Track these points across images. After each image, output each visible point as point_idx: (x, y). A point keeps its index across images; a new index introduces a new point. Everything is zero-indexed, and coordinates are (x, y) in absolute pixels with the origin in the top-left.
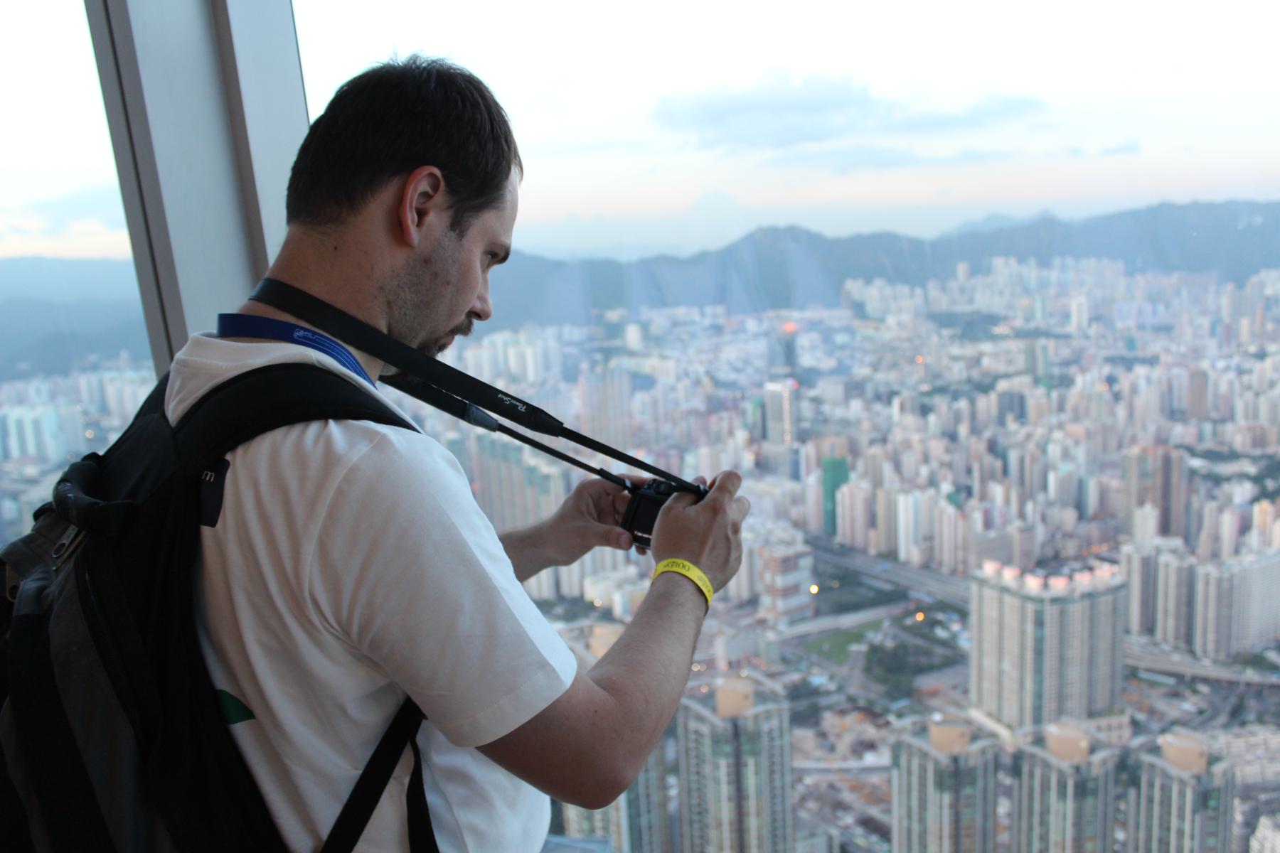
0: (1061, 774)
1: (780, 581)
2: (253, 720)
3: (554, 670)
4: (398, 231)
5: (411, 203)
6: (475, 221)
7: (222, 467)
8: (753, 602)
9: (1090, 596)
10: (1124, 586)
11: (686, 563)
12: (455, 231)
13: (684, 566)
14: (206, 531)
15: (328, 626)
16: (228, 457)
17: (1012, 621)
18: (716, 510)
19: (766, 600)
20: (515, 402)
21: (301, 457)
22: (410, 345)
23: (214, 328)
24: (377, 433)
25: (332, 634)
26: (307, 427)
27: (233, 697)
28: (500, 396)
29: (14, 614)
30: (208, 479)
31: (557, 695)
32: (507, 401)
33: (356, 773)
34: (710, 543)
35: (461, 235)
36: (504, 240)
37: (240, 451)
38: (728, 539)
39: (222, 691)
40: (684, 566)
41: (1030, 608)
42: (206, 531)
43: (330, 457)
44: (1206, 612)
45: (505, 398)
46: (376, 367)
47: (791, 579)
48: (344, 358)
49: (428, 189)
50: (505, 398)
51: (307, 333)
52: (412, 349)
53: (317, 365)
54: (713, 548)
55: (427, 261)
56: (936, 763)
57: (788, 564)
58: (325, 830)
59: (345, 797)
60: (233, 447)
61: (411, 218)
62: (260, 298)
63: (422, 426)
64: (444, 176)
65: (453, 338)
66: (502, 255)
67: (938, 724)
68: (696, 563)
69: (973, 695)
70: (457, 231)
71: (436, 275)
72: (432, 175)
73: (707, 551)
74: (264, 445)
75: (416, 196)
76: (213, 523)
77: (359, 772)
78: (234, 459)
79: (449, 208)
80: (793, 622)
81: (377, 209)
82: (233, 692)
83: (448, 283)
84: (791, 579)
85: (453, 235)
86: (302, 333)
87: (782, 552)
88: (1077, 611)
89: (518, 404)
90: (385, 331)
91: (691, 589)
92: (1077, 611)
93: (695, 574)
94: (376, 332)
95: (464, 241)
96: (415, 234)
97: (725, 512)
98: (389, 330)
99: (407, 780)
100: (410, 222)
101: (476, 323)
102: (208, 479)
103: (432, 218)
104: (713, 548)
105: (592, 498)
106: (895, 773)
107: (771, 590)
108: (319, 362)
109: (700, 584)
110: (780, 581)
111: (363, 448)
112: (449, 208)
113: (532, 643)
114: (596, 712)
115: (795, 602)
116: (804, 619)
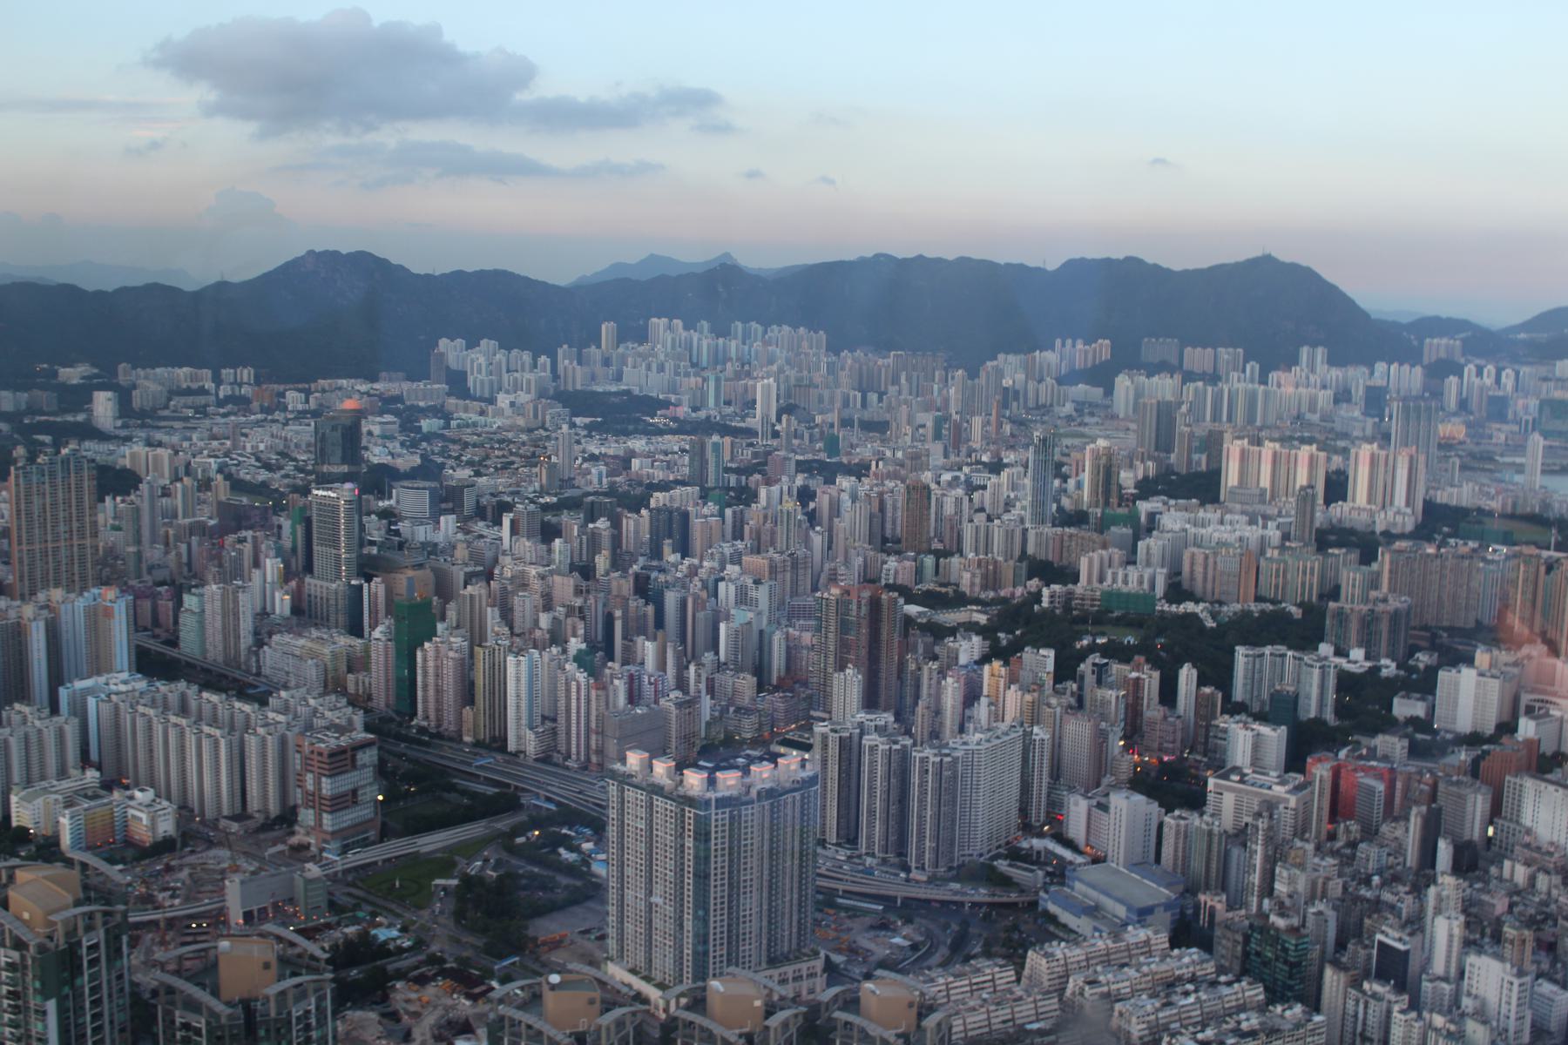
8: (287, 818)
9: (770, 794)
10: (812, 781)
17: (665, 834)
19: (307, 816)
44: (923, 810)
47: (346, 782)
57: (341, 760)
67: (553, 987)
69: (612, 943)
80: (344, 850)
84: (346, 782)
87: (332, 741)
88: (753, 815)
92: (753, 815)
107: (314, 800)
110: (327, 787)
115: (349, 817)
116: (365, 843)
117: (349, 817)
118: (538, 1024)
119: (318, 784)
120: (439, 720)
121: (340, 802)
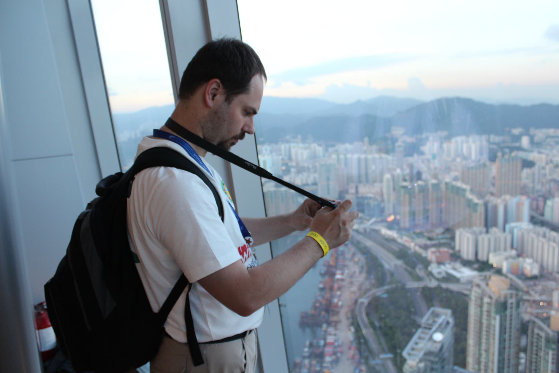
3: (217, 261)
11: (317, 234)
13: (315, 235)
18: (336, 215)
20: (252, 165)
22: (213, 143)
28: (246, 162)
32: (249, 164)
34: (330, 228)
35: (229, 103)
38: (339, 227)
40: (315, 235)
45: (248, 163)
50: (248, 163)
52: (214, 145)
54: (331, 230)
55: (216, 113)
58: (161, 303)
65: (238, 141)
68: (322, 234)
71: (219, 118)
73: (328, 230)
75: (210, 89)
79: (225, 93)
83: (225, 121)
85: (226, 103)
89: (253, 166)
90: (202, 137)
91: (315, 244)
93: (319, 239)
94: (198, 137)
95: (231, 106)
96: (210, 102)
97: (339, 216)
98: (204, 137)
104: (331, 230)
105: (308, 205)
109: (320, 243)
112: (225, 93)
113: (211, 250)
114: (240, 280)
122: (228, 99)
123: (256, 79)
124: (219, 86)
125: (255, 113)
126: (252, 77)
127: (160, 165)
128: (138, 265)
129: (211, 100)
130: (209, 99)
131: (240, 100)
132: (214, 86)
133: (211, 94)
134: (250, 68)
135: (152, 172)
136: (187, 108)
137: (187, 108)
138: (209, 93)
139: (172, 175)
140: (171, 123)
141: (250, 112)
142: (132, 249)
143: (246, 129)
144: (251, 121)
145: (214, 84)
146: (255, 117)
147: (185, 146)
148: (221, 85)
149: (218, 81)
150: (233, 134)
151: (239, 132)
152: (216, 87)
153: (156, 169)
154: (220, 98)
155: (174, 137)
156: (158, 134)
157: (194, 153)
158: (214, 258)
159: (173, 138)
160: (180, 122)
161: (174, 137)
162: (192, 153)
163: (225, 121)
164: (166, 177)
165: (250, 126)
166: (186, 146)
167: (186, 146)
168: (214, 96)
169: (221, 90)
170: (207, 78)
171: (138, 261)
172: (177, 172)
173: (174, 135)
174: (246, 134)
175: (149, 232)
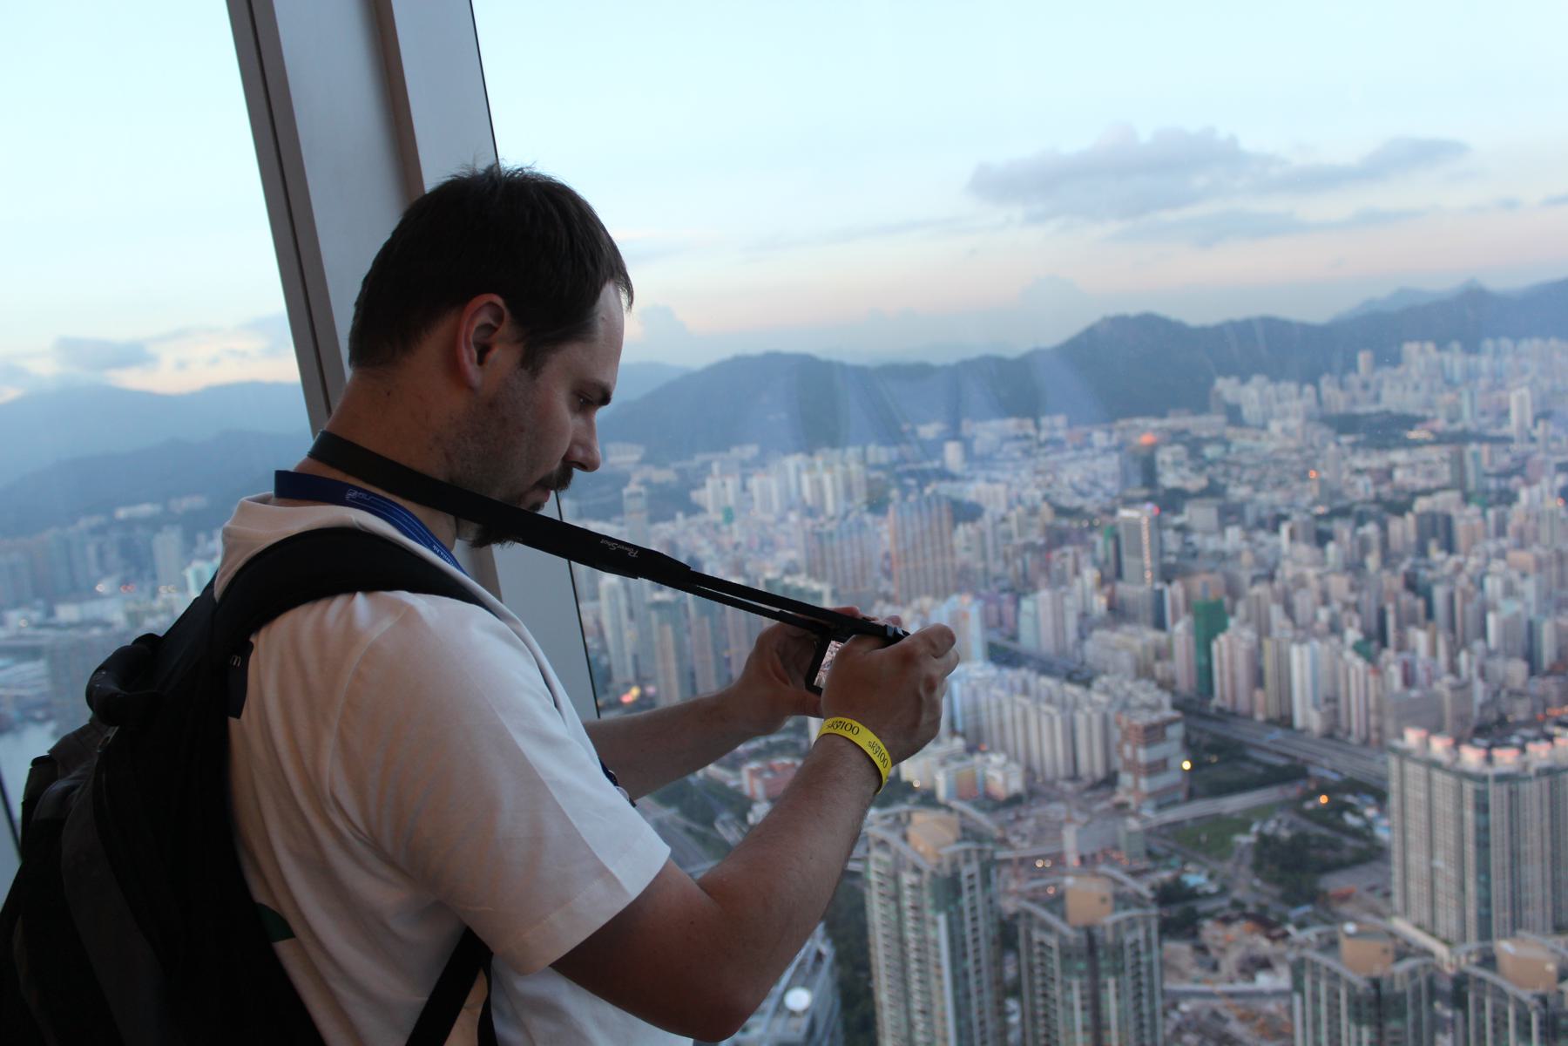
0: (1520, 1003)
1: (1143, 755)
2: (293, 940)
4: (454, 368)
5: (467, 336)
6: (553, 355)
7: (246, 649)
8: (1110, 781)
9: (1550, 772)
12: (526, 369)
14: (233, 721)
15: (359, 835)
16: (253, 639)
17: (1444, 805)
19: (1126, 779)
21: (320, 636)
23: (270, 491)
24: (402, 604)
25: (360, 840)
26: (328, 606)
27: (269, 910)
29: (33, 819)
30: (235, 663)
31: (619, 906)
33: (420, 999)
36: (602, 377)
37: (263, 632)
39: (261, 904)
41: (1469, 787)
42: (233, 721)
43: (351, 633)
46: (441, 524)
47: (1158, 752)
48: (403, 522)
49: (491, 321)
51: (360, 494)
53: (360, 528)
56: (1351, 986)
57: (1153, 734)
59: (409, 1028)
60: (256, 628)
61: (468, 356)
62: (317, 454)
63: (497, 593)
64: (507, 305)
66: (598, 396)
67: (1349, 936)
69: (1397, 900)
70: (530, 369)
72: (491, 304)
74: (283, 625)
76: (238, 716)
77: (425, 999)
78: (257, 641)
80: (1160, 807)
81: (430, 349)
82: (272, 907)
84: (1158, 752)
86: (355, 494)
87: (1144, 718)
88: (1532, 792)
92: (1532, 792)
99: (479, 1011)
100: (466, 360)
101: (577, 473)
102: (235, 663)
103: (496, 354)
106: (1297, 998)
107: (1132, 766)
108: (360, 525)
110: (1143, 755)
111: (387, 623)
115: (1162, 781)
117: (1162, 781)
118: (1336, 966)
119: (1134, 753)
120: (1234, 701)
121: (1156, 768)
122: (531, 362)
123: (609, 293)
124: (499, 318)
125: (605, 399)
126: (601, 288)
127: (351, 589)
128: (284, 948)
129: (476, 365)
130: (471, 359)
131: (565, 360)
132: (485, 318)
133: (476, 344)
134: (593, 259)
135: (324, 613)
136: (389, 394)
137: (389, 394)
138: (471, 341)
139: (409, 617)
140: (329, 448)
141: (592, 396)
142: (260, 896)
143: (579, 454)
144: (590, 426)
145: (483, 310)
146: (601, 414)
147: (393, 515)
148: (507, 313)
149: (498, 300)
150: (539, 474)
151: (556, 465)
152: (491, 321)
153: (339, 602)
154: (504, 356)
155: (364, 496)
156: (292, 487)
157: (433, 544)
158: (603, 872)
159: (358, 499)
160: (368, 439)
161: (364, 496)
162: (429, 543)
163: (522, 430)
164: (387, 623)
165: (588, 447)
166: (395, 513)
167: (395, 513)
168: (483, 351)
169: (505, 329)
170: (459, 295)
171: (288, 933)
172: (423, 604)
173: (359, 490)
174: (577, 472)
175: (340, 823)
